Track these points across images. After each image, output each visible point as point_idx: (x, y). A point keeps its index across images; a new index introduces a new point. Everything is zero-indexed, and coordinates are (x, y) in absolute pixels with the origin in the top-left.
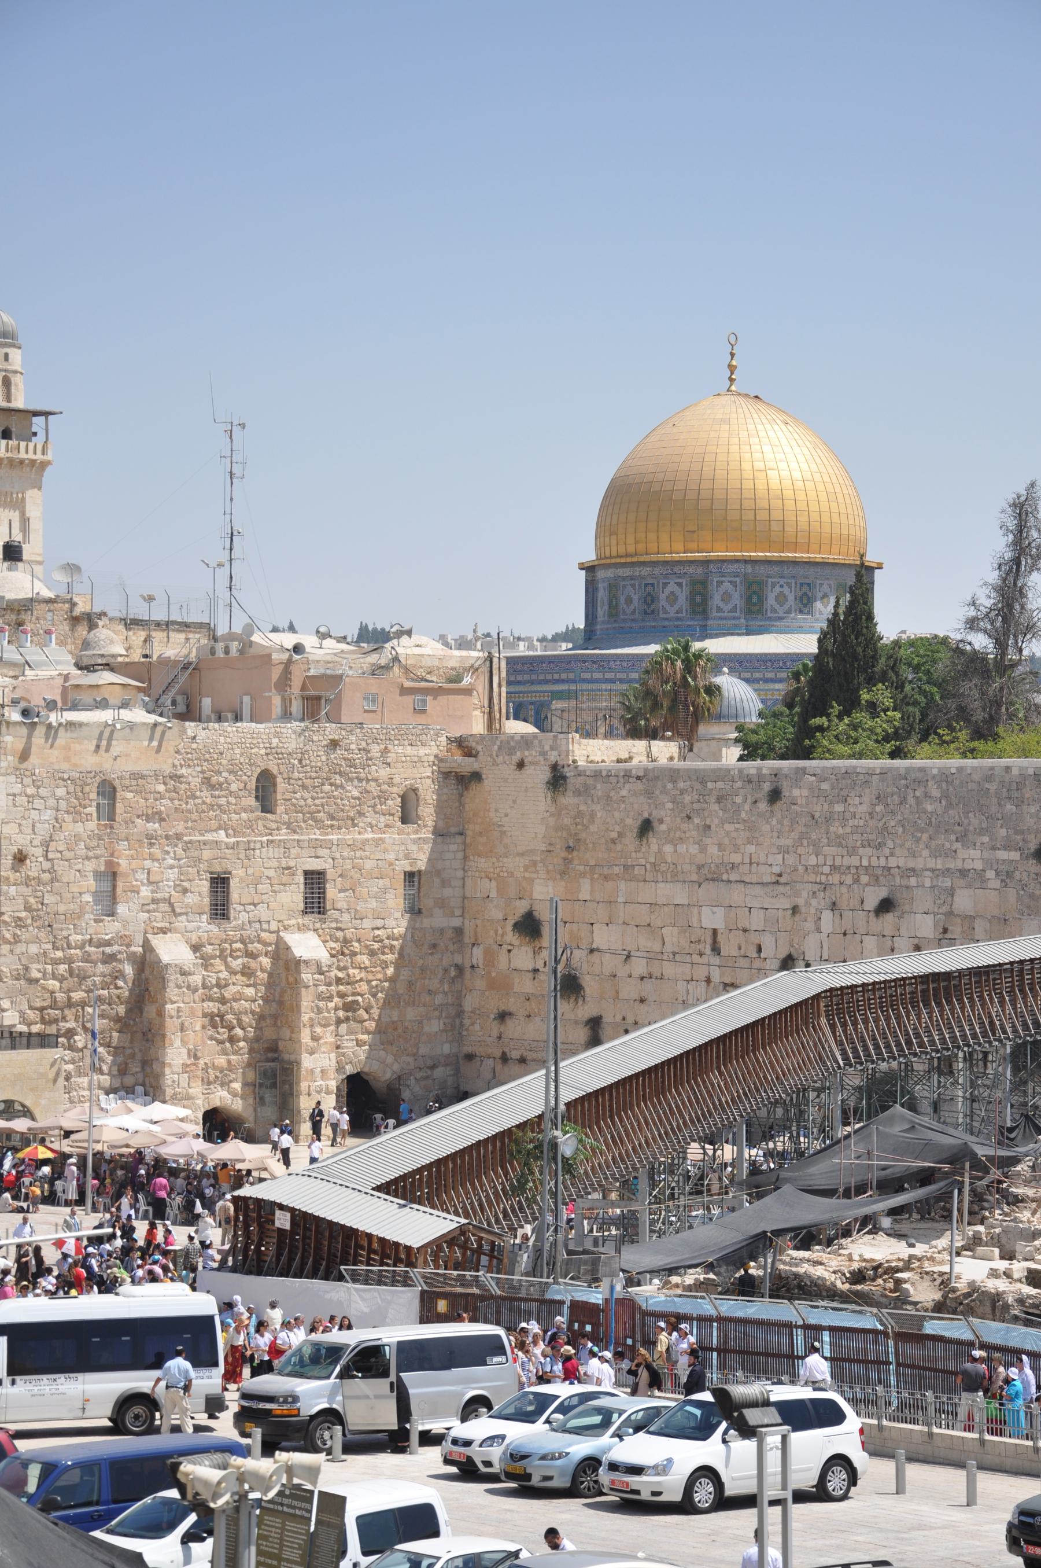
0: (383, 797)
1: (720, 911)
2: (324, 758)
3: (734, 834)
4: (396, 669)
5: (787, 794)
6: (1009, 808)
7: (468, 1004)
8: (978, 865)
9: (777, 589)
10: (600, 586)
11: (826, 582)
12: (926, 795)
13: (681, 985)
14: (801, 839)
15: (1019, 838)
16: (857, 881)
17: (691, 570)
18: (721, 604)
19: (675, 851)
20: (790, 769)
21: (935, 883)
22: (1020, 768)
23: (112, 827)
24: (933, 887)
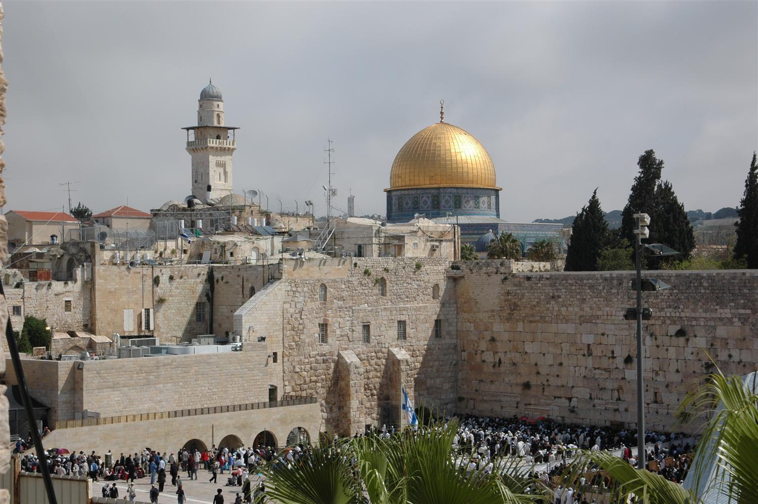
0: (426, 288)
3: (598, 303)
4: (420, 233)
6: (746, 291)
7: (460, 376)
8: (729, 316)
9: (466, 199)
12: (701, 284)
13: (572, 369)
16: (664, 322)
17: (433, 191)
19: (567, 310)
21: (706, 324)
22: (750, 273)
23: (325, 304)
24: (705, 326)
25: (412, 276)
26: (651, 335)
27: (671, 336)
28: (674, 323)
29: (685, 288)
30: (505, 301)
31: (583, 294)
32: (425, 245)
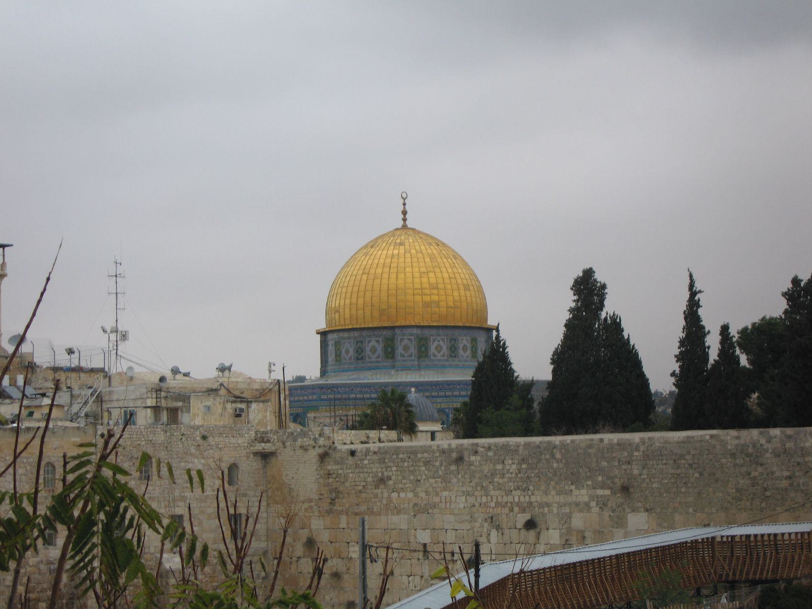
1: (428, 531)
2: (181, 446)
3: (435, 485)
4: (223, 392)
5: (467, 459)
6: (604, 464)
8: (586, 499)
9: (436, 343)
10: (330, 343)
11: (465, 338)
12: (553, 456)
13: (405, 578)
14: (476, 486)
15: (609, 482)
18: (403, 352)
19: (399, 496)
20: (469, 444)
22: (609, 440)
24: (558, 513)
25: (193, 451)
26: (498, 528)
27: (520, 529)
28: (523, 510)
29: (535, 462)
30: (325, 486)
31: (417, 473)
32: (225, 408)
